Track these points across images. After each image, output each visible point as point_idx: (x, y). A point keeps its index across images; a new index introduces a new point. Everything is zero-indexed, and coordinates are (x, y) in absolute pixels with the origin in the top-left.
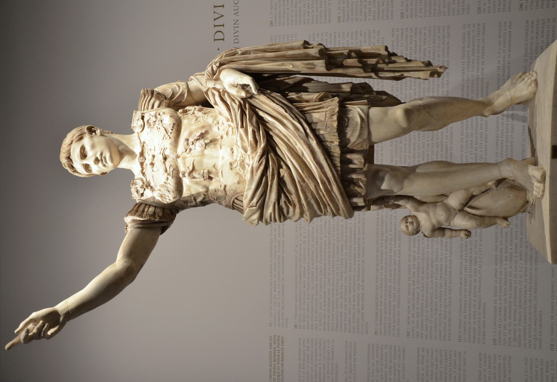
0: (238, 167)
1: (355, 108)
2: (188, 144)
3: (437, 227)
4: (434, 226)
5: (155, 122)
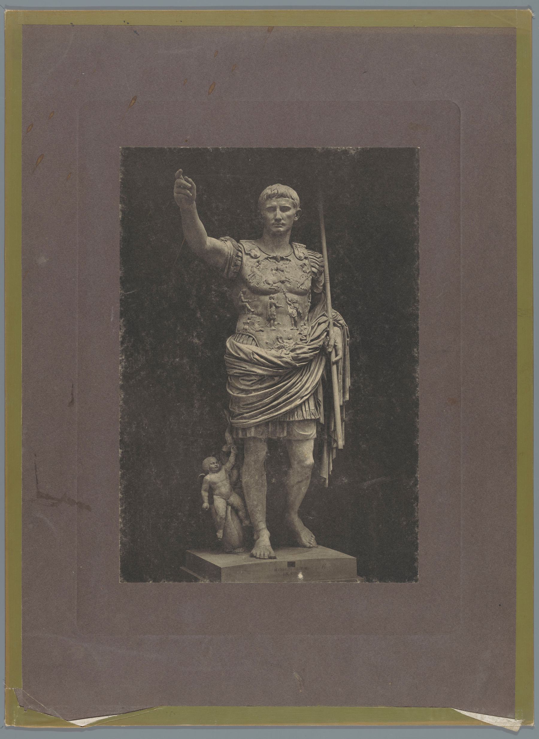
0: (279, 344)
4: (215, 483)
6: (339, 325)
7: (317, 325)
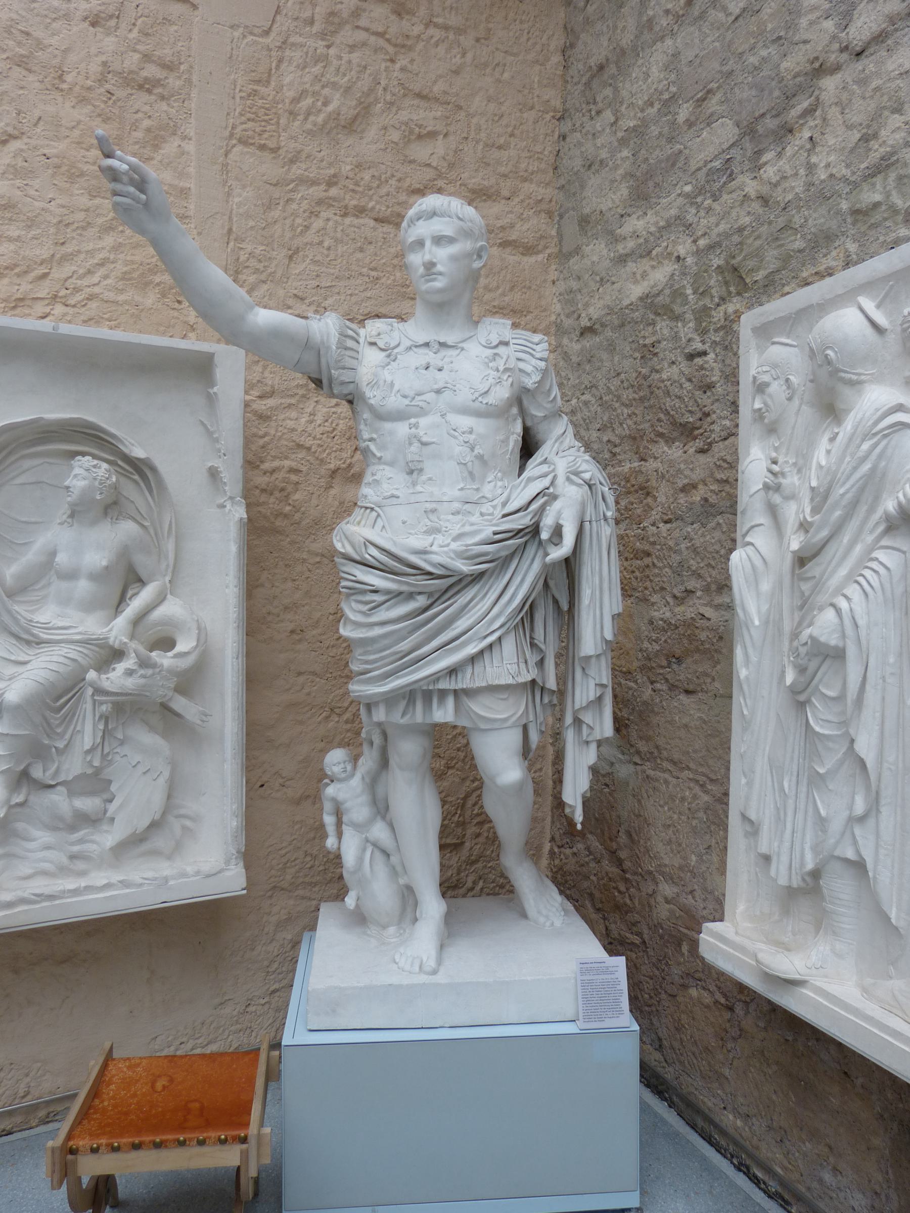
0: (429, 523)
4: (342, 804)
5: (498, 370)
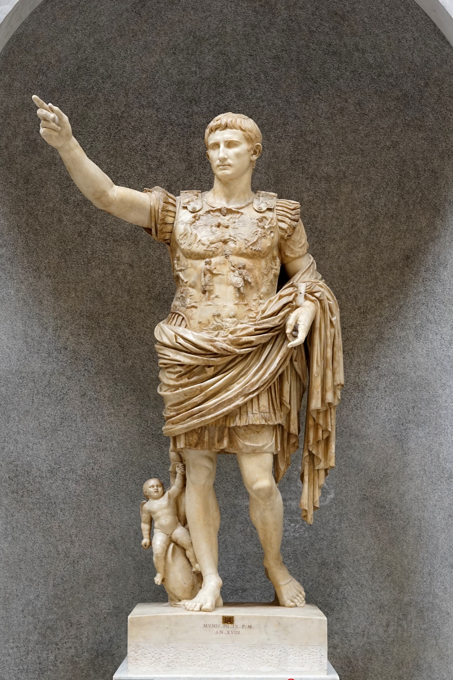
0: (215, 323)
1: (272, 441)
2: (240, 268)
3: (154, 516)
4: (154, 513)
5: (264, 228)
6: (314, 298)
7: (277, 298)
